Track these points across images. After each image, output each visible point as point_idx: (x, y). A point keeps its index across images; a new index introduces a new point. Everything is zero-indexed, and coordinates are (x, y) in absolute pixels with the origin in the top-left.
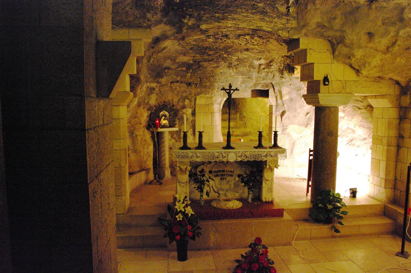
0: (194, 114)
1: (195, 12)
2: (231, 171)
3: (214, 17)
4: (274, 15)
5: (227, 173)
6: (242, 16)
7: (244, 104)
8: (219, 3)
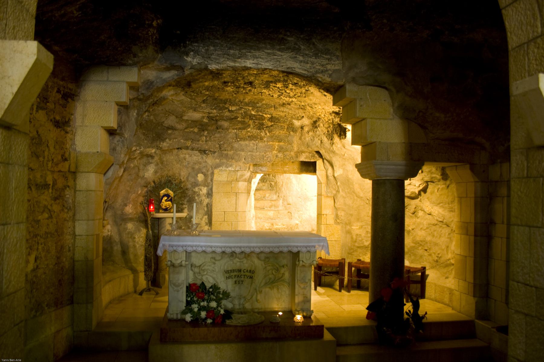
0: (210, 194)
1: (202, 48)
2: (250, 271)
4: (310, 54)
5: (244, 274)
6: (266, 53)
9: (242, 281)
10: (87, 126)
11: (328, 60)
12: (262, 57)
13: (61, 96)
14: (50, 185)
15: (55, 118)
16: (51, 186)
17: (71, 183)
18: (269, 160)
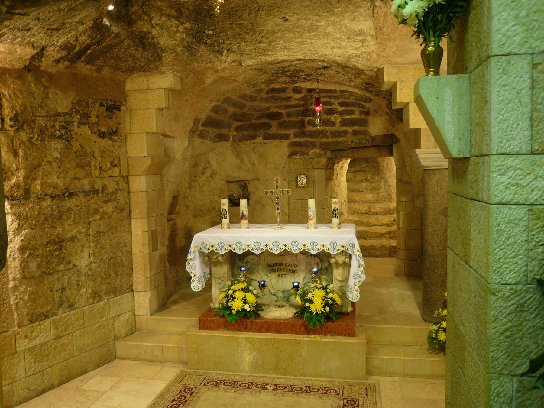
2: (292, 265)
3: (259, 48)
4: (342, 37)
7: (389, 167)
8: (263, 28)
10: (134, 133)
11: (363, 42)
12: (292, 47)
13: (105, 109)
14: (99, 190)
15: (99, 131)
16: (100, 191)
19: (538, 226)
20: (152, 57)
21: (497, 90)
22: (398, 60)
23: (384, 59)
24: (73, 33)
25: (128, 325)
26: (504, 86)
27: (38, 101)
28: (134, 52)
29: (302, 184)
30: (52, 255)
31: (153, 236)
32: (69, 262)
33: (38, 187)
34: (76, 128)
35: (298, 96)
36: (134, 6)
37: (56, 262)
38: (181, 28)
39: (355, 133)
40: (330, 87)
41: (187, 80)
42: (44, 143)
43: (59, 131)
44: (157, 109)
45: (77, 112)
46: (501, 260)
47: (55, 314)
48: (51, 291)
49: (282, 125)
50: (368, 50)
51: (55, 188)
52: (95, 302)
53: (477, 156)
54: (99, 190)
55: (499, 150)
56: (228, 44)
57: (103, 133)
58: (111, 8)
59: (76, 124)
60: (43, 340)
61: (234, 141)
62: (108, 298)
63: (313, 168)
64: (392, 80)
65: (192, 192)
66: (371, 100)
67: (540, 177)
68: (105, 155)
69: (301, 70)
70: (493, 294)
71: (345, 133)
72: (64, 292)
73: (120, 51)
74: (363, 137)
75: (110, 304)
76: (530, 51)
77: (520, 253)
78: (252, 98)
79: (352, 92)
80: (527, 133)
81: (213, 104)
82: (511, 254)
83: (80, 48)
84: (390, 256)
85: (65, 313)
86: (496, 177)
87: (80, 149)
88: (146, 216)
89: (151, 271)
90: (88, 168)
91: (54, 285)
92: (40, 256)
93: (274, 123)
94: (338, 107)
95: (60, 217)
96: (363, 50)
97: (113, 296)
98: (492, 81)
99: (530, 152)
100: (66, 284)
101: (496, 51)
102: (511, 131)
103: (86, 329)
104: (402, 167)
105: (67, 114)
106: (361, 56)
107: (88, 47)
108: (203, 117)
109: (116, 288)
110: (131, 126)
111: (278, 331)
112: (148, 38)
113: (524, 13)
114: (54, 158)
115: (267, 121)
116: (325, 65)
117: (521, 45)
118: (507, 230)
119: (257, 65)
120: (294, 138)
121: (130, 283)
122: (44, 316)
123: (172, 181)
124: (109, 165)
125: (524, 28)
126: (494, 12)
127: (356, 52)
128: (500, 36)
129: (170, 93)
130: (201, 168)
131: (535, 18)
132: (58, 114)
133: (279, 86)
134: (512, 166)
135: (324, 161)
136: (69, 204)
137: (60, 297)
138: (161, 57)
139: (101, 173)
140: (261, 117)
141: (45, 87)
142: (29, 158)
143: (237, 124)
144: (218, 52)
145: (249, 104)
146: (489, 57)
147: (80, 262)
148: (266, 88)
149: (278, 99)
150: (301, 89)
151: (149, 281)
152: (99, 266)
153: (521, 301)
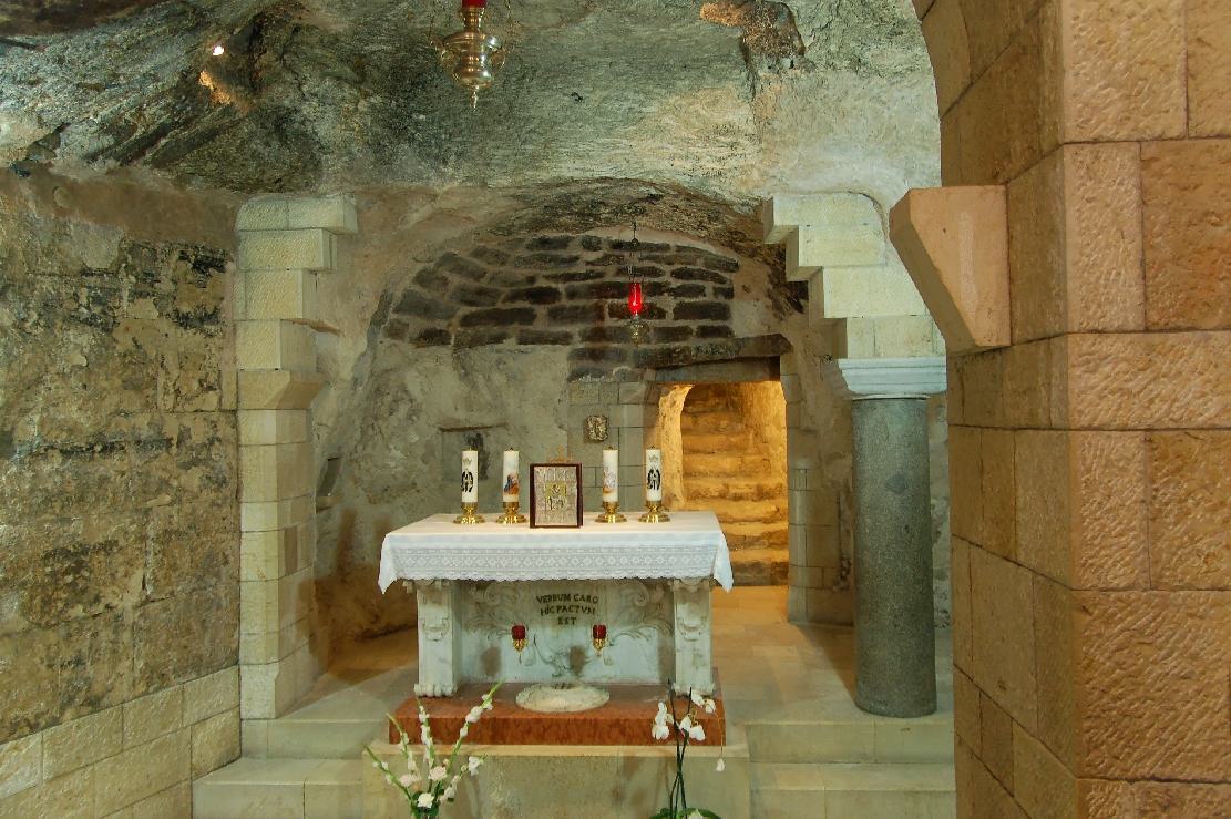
2: (589, 597)
5: (577, 603)
9: (573, 619)
10: (252, 320)
13: (190, 266)
14: (172, 439)
15: (177, 311)
16: (174, 442)
17: (225, 430)
18: (681, 357)
19: (1164, 471)
20: (299, 159)
21: (1077, 208)
22: (801, 184)
23: (775, 181)
24: (133, 97)
25: (224, 743)
26: (1089, 201)
27: (42, 242)
28: (260, 148)
29: (598, 435)
30: (56, 583)
31: (289, 540)
32: (97, 599)
33: (34, 430)
34: (125, 303)
35: (592, 256)
36: (265, 52)
37: (66, 600)
38: (363, 106)
39: (705, 332)
40: (657, 240)
41: (368, 214)
42: (52, 332)
43: (88, 308)
44: (304, 270)
45: (130, 269)
46: (1096, 542)
47: (55, 722)
48: (50, 666)
49: (555, 315)
50: (742, 162)
51: (71, 431)
52: (151, 689)
53: (1030, 341)
54: (172, 439)
55: (1085, 324)
56: (460, 142)
57: (186, 317)
58: (219, 51)
59: (125, 294)
60: (22, 784)
61: (458, 345)
62: (181, 680)
63: (619, 402)
64: (789, 222)
65: (369, 450)
66: (736, 265)
67: (1164, 376)
68: (187, 365)
69: (602, 203)
70: (1085, 610)
71: (683, 333)
72: (80, 667)
73: (231, 145)
74: (720, 340)
75: (185, 694)
76: (1136, 136)
77: (1132, 525)
78: (500, 258)
79: (701, 251)
80: (1136, 291)
81: (419, 267)
82: (1115, 528)
83: (144, 133)
84: (773, 583)
85: (80, 716)
86: (1080, 376)
87: (134, 349)
88: (273, 495)
89: (281, 613)
90: (150, 392)
91: (57, 653)
92: (29, 586)
93: (541, 310)
94: (671, 280)
95: (81, 499)
96: (732, 162)
97: (194, 676)
98: (1067, 192)
99: (1142, 329)
100: (85, 650)
101: (1072, 135)
102: (1105, 287)
103: (127, 753)
104: (795, 402)
105: (106, 271)
106: (729, 175)
107: (162, 131)
108: (398, 294)
109: (200, 657)
110: (246, 306)
111: (564, 739)
112: (293, 121)
113: (1121, 64)
114: (73, 366)
115: (525, 304)
116: (653, 192)
117: (1120, 122)
118: (1106, 481)
119: (519, 188)
120: (581, 342)
121: (234, 646)
122: (29, 725)
123: (330, 424)
124: (195, 385)
125: (1123, 91)
126: (1067, 61)
127: (718, 167)
128: (1080, 105)
129: (334, 238)
130: (389, 399)
131: (1142, 75)
132: (86, 272)
133: (555, 235)
134: (1110, 355)
135: (640, 388)
136: (102, 468)
137: (69, 682)
138: (319, 162)
139: (176, 404)
140: (514, 297)
141: (61, 212)
142: (14, 365)
143: (465, 310)
144: (436, 158)
145: (492, 269)
146: (1058, 146)
147: (122, 599)
148: (530, 237)
149: (550, 261)
150: (599, 241)
151: (276, 641)
152: (165, 609)
153: (1139, 623)
